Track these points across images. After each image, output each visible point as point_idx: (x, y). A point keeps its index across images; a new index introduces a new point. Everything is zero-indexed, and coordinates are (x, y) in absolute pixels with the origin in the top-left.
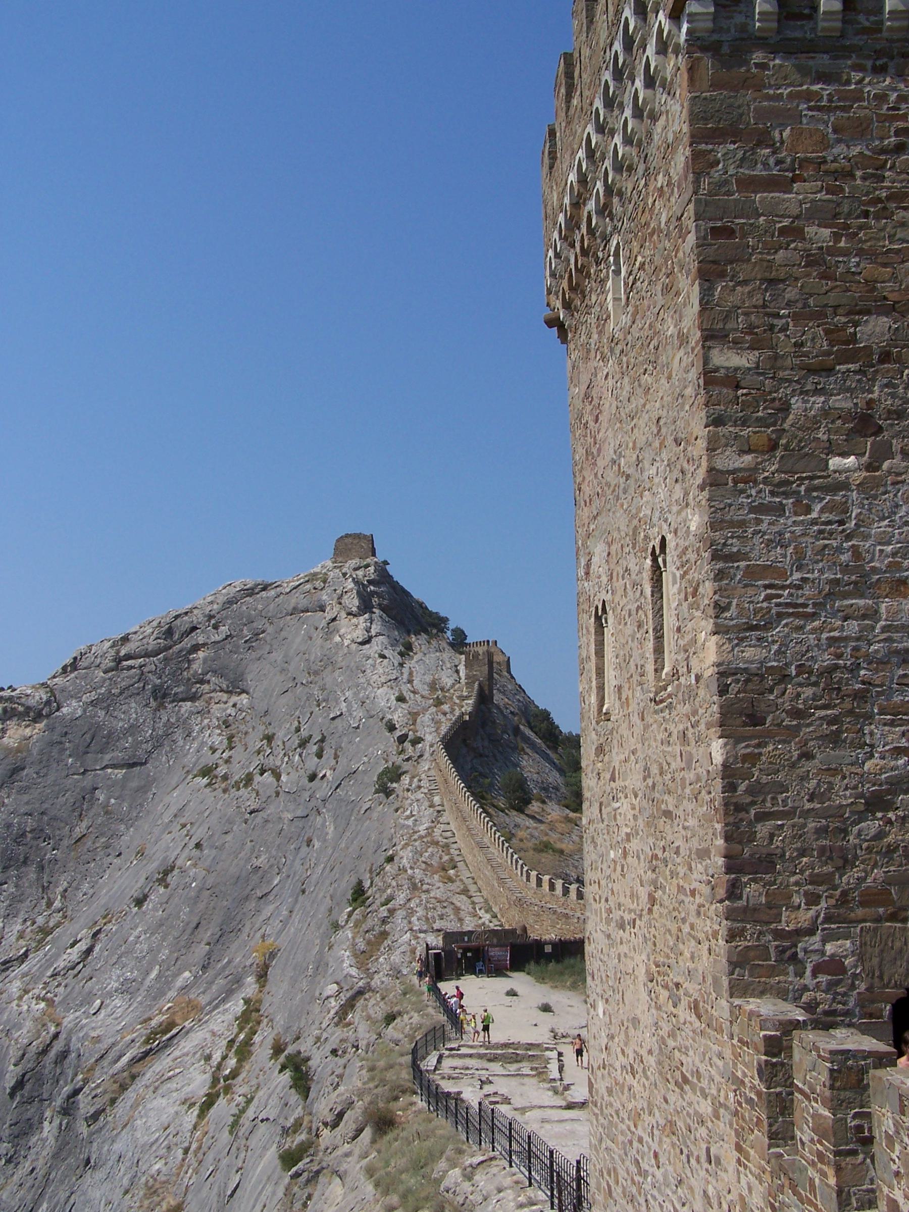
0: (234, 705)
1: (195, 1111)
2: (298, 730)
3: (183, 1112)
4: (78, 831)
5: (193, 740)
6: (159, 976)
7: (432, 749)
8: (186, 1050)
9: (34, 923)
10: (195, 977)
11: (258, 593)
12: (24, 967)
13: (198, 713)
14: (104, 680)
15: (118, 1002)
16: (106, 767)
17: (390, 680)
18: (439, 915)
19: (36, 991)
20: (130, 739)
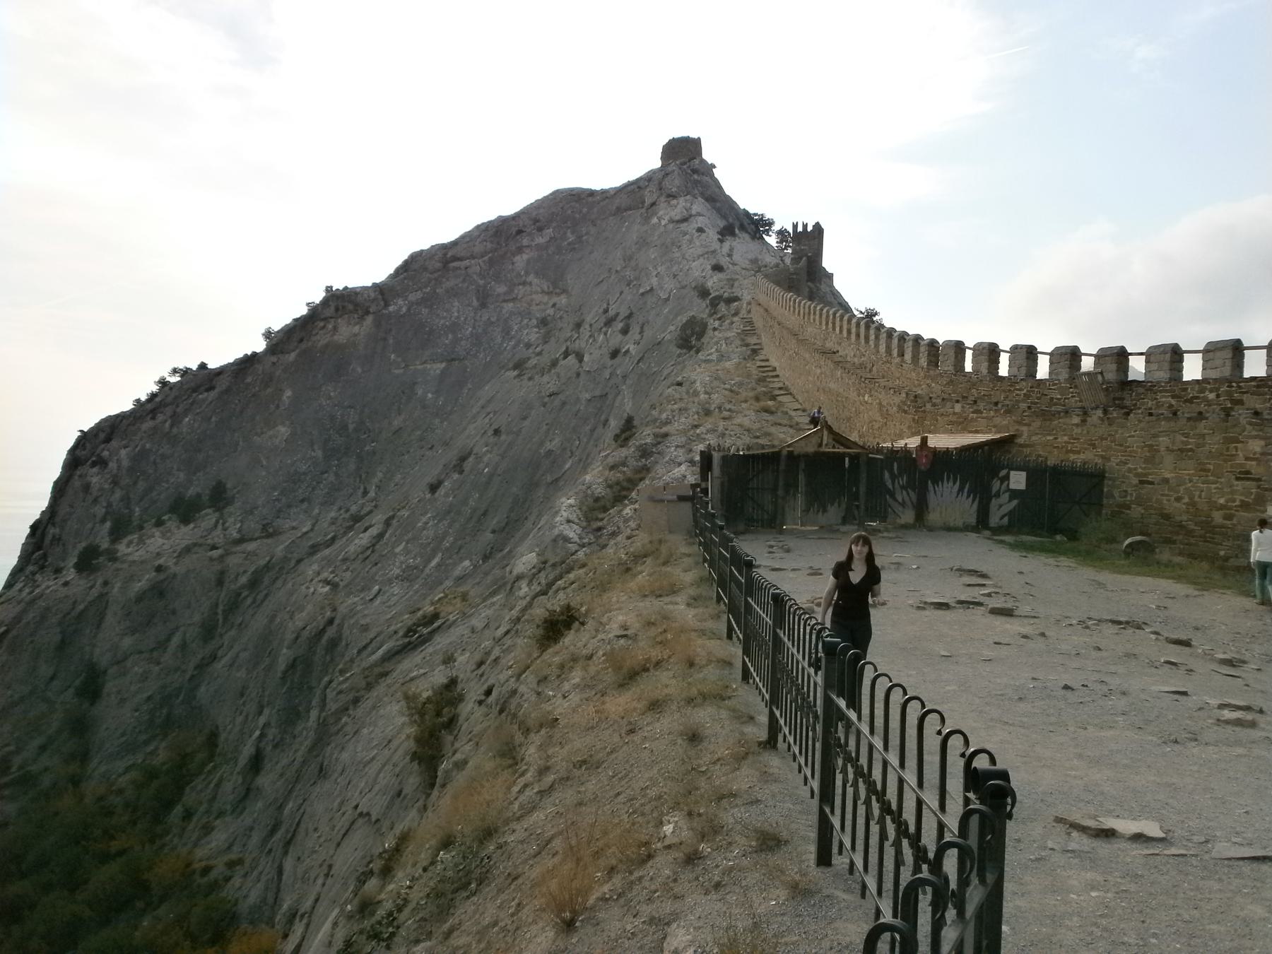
0: (554, 305)
2: (606, 311)
4: (397, 423)
5: (512, 338)
6: (439, 565)
10: (475, 566)
11: (583, 199)
12: (327, 552)
13: (520, 313)
16: (425, 362)
17: (707, 253)
19: (325, 575)
20: (450, 336)
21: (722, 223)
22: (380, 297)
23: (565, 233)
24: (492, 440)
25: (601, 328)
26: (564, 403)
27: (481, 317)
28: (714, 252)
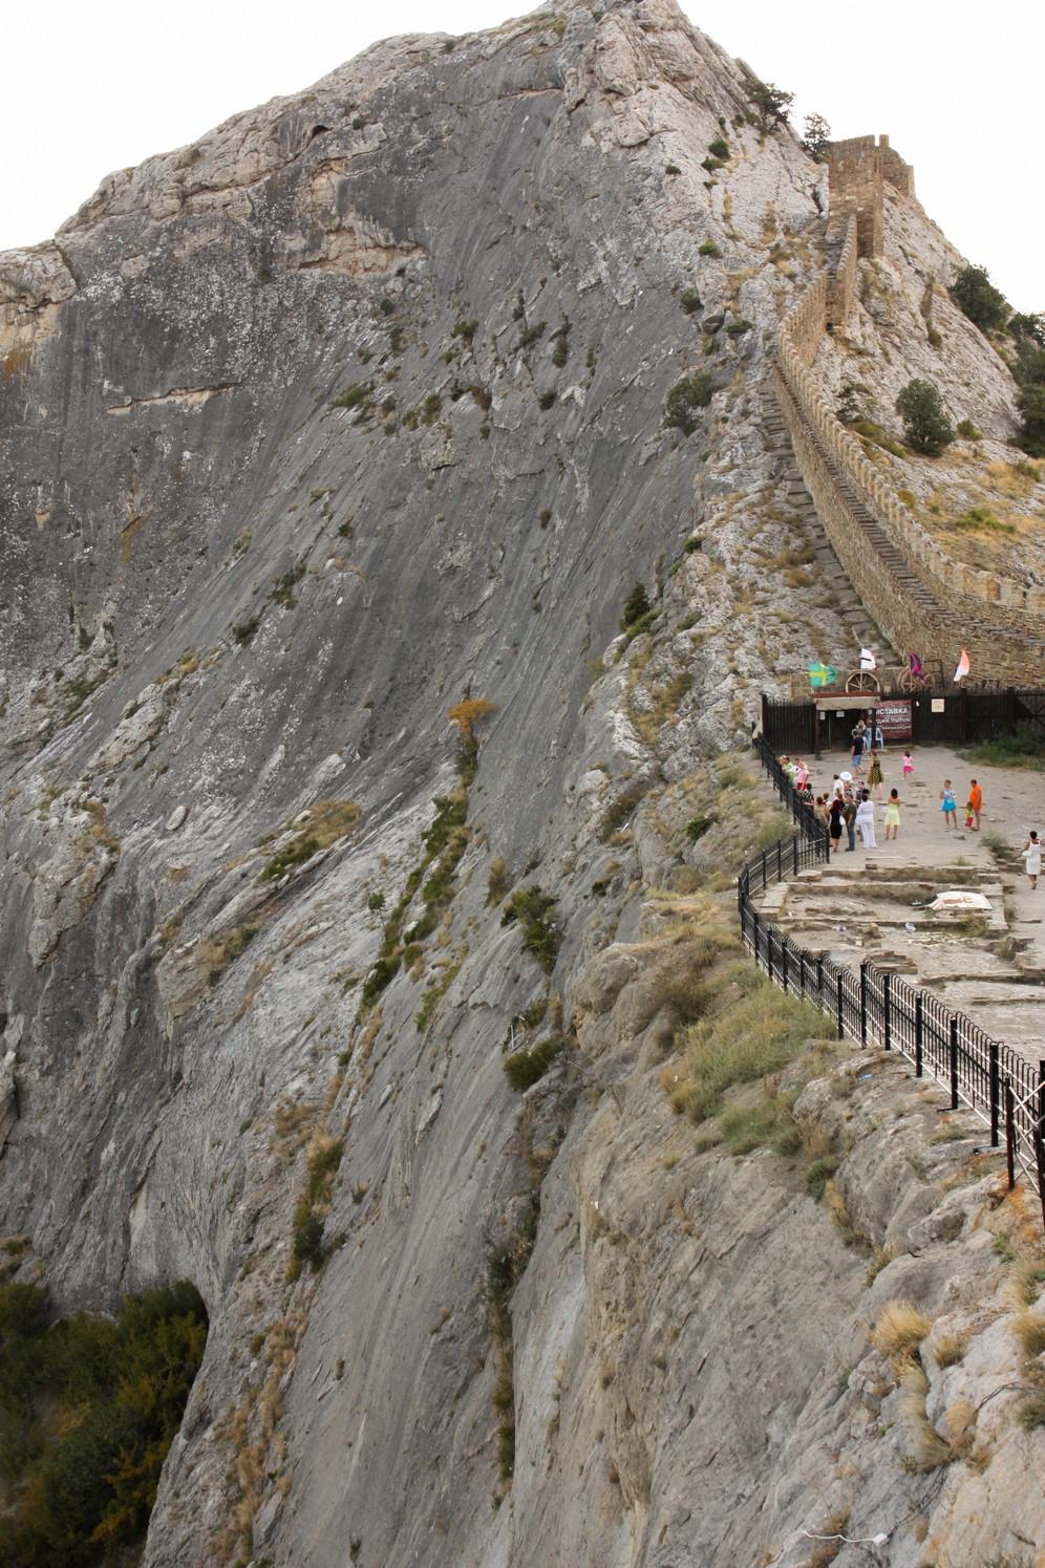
0: (401, 272)
1: (358, 994)
2: (519, 314)
3: (337, 995)
4: (131, 505)
5: (327, 339)
6: (285, 765)
7: (768, 344)
8: (336, 890)
9: (59, 675)
10: (349, 764)
14: (158, 233)
15: (214, 810)
18: (785, 646)
19: (72, 793)
20: (213, 341)
21: (706, 131)
22: (65, 269)
23: (408, 131)
24: (342, 544)
25: (516, 350)
26: (467, 484)
27: (265, 300)
28: (699, 215)
